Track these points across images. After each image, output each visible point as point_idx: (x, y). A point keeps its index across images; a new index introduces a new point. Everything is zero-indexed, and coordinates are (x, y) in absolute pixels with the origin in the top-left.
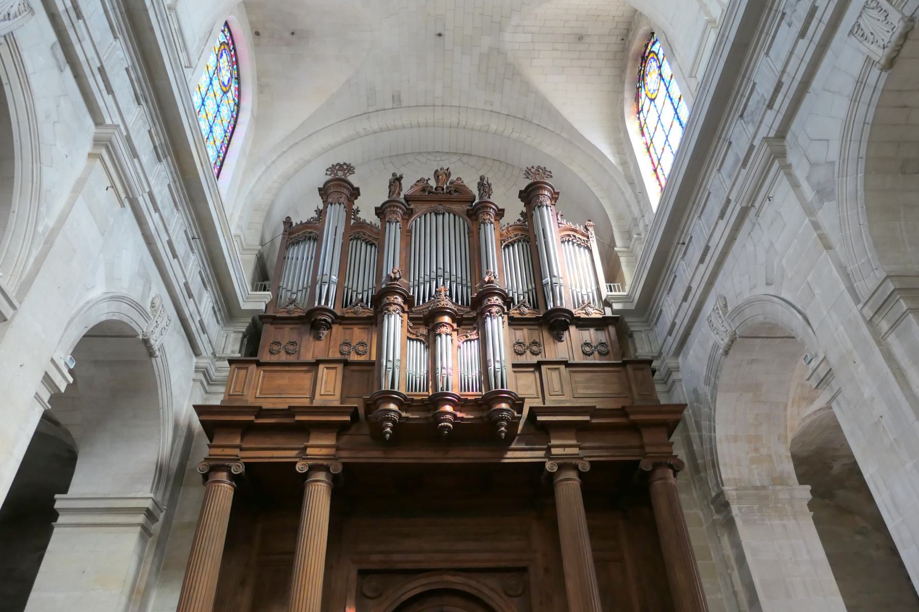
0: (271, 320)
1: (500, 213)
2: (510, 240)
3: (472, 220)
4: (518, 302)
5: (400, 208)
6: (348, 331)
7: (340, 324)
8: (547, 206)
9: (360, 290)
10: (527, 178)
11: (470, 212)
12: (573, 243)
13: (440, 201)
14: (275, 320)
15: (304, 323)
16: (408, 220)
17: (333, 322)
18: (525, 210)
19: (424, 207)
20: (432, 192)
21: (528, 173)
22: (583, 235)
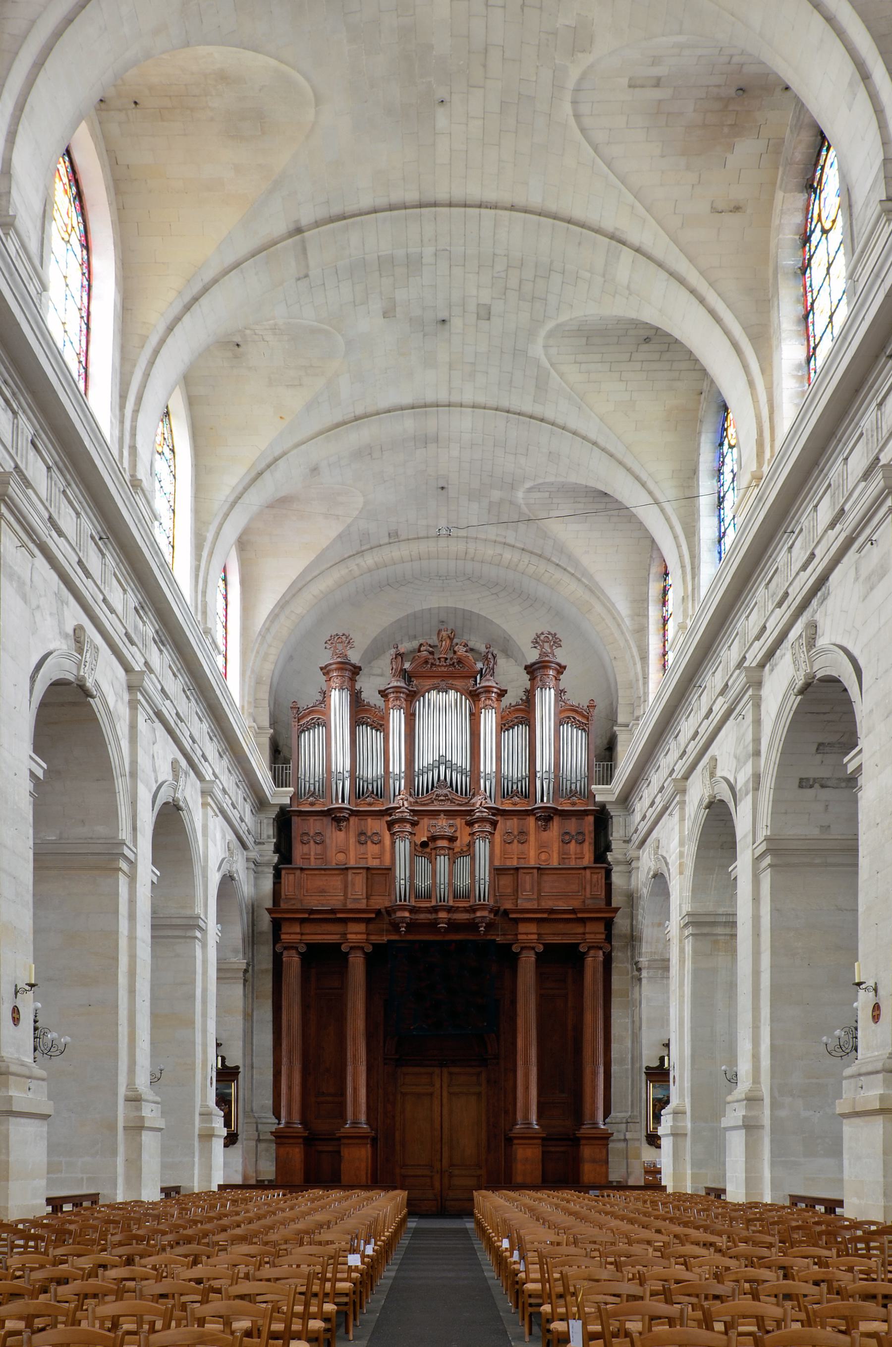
0: (298, 814)
1: (502, 693)
2: (511, 724)
3: (474, 701)
4: (512, 793)
5: (403, 693)
6: (363, 822)
7: (356, 816)
8: (550, 689)
9: (370, 781)
10: (535, 647)
11: (473, 693)
12: (572, 726)
13: (444, 677)
14: (301, 813)
15: (325, 816)
16: (411, 702)
17: (350, 815)
18: (529, 687)
19: (428, 683)
20: (435, 665)
21: (537, 642)
22: (583, 716)
